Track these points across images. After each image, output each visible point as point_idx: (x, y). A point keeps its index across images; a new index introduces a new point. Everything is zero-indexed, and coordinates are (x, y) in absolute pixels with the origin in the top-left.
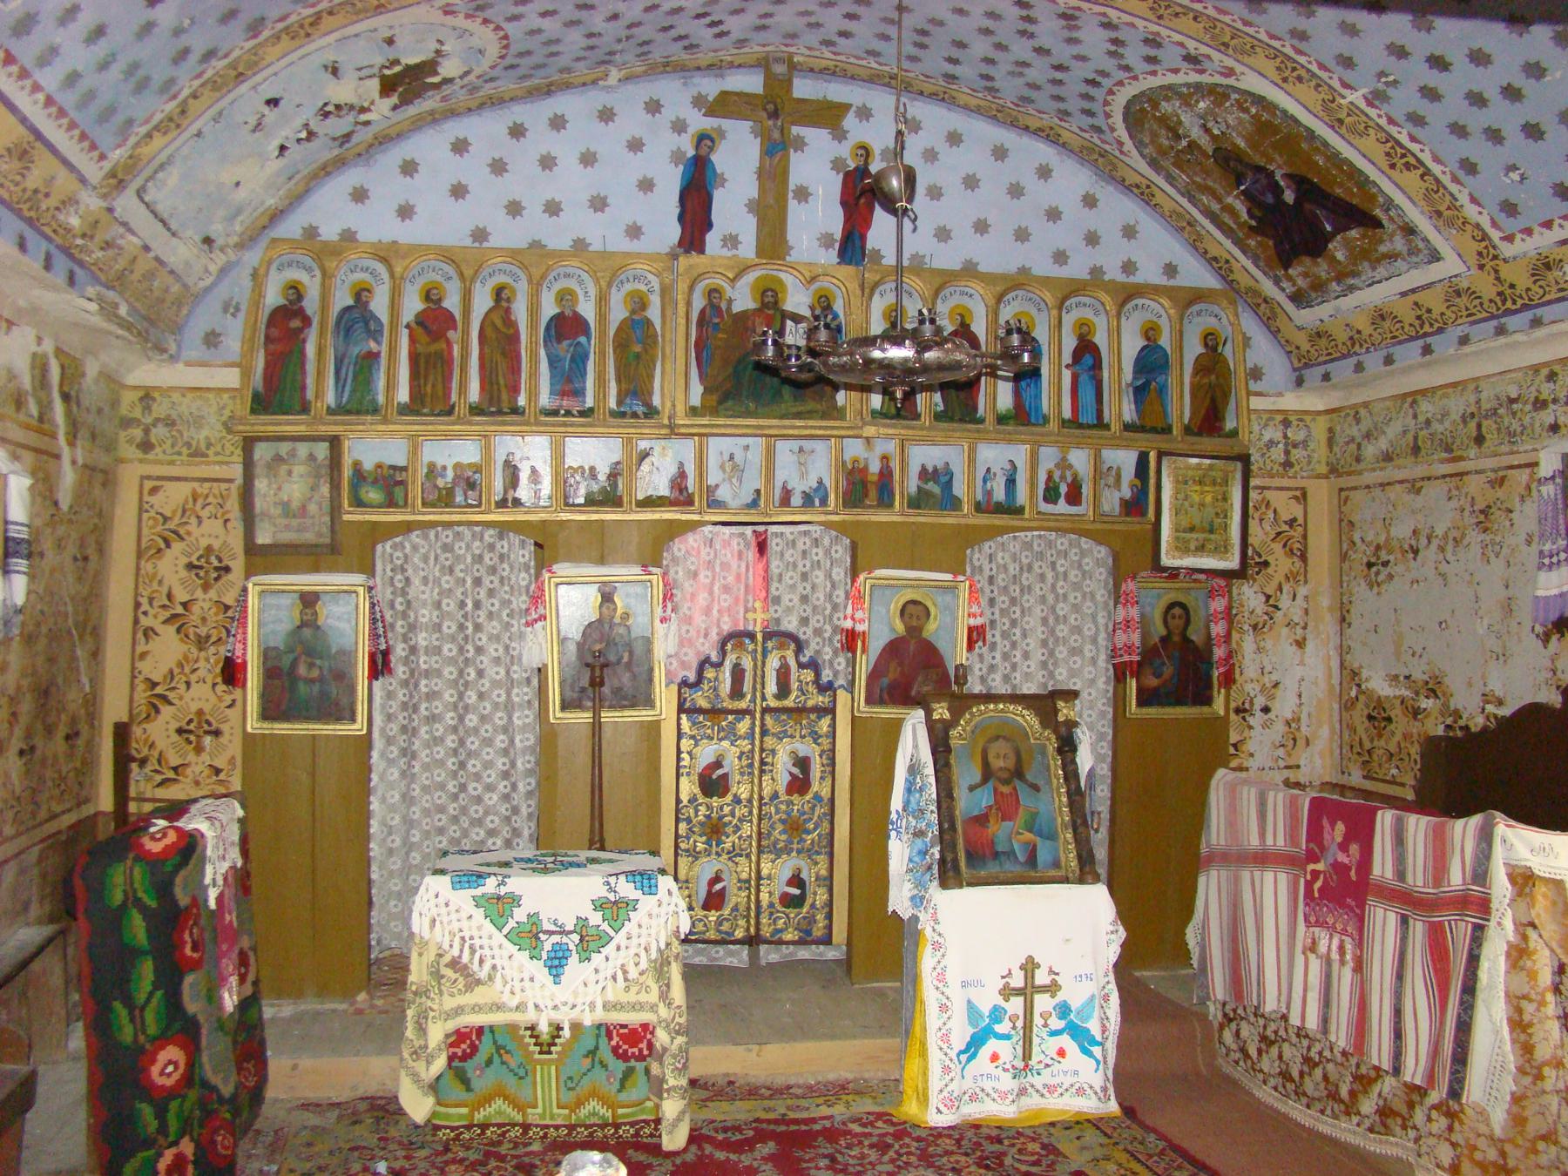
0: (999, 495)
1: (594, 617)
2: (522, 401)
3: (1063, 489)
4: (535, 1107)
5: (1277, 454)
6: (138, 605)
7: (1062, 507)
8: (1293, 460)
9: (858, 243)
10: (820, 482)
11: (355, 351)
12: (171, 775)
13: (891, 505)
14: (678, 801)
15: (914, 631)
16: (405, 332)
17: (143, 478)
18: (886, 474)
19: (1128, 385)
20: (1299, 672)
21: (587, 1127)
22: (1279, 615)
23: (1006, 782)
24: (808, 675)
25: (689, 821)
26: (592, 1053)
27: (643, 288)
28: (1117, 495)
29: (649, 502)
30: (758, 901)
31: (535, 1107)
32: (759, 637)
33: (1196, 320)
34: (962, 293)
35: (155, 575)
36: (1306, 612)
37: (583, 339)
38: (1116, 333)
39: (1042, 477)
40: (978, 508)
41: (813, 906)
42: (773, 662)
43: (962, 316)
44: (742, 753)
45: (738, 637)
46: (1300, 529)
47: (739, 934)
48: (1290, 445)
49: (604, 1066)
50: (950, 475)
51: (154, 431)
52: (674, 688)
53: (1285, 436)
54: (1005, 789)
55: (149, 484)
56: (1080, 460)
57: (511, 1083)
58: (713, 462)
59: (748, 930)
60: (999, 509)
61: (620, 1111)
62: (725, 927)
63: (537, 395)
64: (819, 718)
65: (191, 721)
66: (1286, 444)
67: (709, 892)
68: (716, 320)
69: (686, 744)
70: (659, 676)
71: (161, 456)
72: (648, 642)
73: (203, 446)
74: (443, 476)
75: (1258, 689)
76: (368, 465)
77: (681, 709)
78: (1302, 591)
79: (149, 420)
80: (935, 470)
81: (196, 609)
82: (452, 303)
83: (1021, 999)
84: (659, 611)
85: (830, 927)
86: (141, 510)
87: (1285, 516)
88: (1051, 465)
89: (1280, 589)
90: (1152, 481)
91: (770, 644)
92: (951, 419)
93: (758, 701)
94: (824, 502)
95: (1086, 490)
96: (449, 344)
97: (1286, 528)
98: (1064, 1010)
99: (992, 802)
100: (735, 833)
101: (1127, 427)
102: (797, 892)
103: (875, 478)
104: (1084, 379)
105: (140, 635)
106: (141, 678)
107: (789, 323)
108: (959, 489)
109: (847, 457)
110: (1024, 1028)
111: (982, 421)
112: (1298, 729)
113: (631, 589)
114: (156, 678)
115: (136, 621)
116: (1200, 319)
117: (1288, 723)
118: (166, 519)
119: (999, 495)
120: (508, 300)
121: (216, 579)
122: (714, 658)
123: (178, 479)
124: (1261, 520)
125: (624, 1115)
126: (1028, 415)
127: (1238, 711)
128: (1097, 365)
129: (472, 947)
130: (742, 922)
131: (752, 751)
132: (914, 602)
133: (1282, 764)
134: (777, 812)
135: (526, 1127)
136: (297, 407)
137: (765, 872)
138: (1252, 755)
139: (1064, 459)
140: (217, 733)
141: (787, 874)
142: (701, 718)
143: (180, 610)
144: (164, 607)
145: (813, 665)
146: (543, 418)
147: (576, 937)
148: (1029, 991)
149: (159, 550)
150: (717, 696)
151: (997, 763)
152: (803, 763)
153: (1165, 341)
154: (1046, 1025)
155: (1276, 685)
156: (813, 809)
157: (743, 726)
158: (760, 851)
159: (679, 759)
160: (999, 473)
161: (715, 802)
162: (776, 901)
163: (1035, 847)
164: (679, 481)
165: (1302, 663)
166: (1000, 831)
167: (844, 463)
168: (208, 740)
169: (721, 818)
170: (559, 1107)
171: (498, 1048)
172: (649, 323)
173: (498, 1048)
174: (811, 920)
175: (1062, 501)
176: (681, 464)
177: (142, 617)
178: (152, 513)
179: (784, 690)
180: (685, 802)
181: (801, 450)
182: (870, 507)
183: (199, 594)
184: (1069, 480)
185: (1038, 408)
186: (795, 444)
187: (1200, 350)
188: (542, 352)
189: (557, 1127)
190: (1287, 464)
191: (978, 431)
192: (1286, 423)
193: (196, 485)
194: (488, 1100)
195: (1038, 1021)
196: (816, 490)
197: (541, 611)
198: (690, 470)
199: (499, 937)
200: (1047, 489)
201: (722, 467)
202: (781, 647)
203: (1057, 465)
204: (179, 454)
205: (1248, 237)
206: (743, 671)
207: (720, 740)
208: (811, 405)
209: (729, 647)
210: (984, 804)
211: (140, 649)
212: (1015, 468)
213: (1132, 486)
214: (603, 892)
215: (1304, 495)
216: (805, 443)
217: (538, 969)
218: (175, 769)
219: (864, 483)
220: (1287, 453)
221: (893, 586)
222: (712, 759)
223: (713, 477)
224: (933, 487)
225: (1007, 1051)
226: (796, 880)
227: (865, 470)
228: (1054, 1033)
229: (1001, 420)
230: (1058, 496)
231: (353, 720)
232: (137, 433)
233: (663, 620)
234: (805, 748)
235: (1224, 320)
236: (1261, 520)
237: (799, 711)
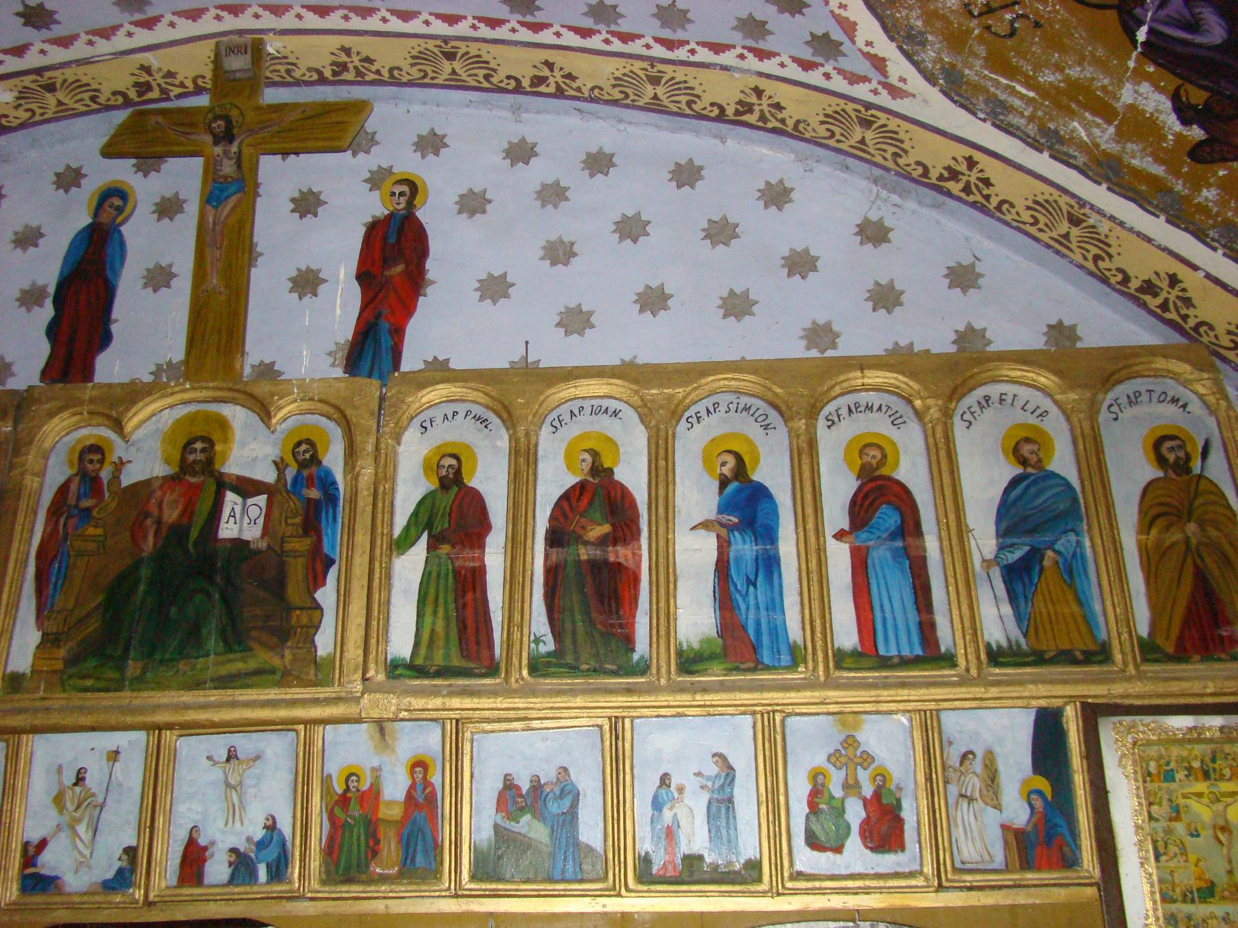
3: (855, 813)
7: (856, 856)
9: (386, 341)
10: (272, 827)
13: (434, 874)
28: (992, 819)
33: (1129, 413)
34: (595, 411)
39: (799, 790)
40: (647, 875)
43: (595, 454)
50: (569, 791)
68: (86, 503)
80: (537, 786)
88: (820, 760)
90: (1079, 780)
92: (574, 670)
94: (278, 871)
95: (912, 812)
101: (996, 656)
103: (396, 813)
104: (881, 555)
107: (230, 497)
108: (591, 830)
109: (334, 767)
111: (643, 668)
116: (1135, 410)
126: (755, 649)
128: (910, 527)
139: (850, 742)
153: (1062, 462)
160: (691, 784)
167: (326, 780)
175: (854, 843)
181: (232, 756)
182: (384, 879)
184: (868, 791)
185: (778, 631)
186: (218, 744)
187: (1149, 472)
196: (261, 845)
201: (59, 800)
203: (833, 758)
205: (1197, 184)
208: (262, 657)
212: (729, 770)
213: (1030, 795)
216: (239, 740)
219: (372, 826)
224: (531, 828)
227: (372, 796)
229: (690, 662)
235: (1196, 407)
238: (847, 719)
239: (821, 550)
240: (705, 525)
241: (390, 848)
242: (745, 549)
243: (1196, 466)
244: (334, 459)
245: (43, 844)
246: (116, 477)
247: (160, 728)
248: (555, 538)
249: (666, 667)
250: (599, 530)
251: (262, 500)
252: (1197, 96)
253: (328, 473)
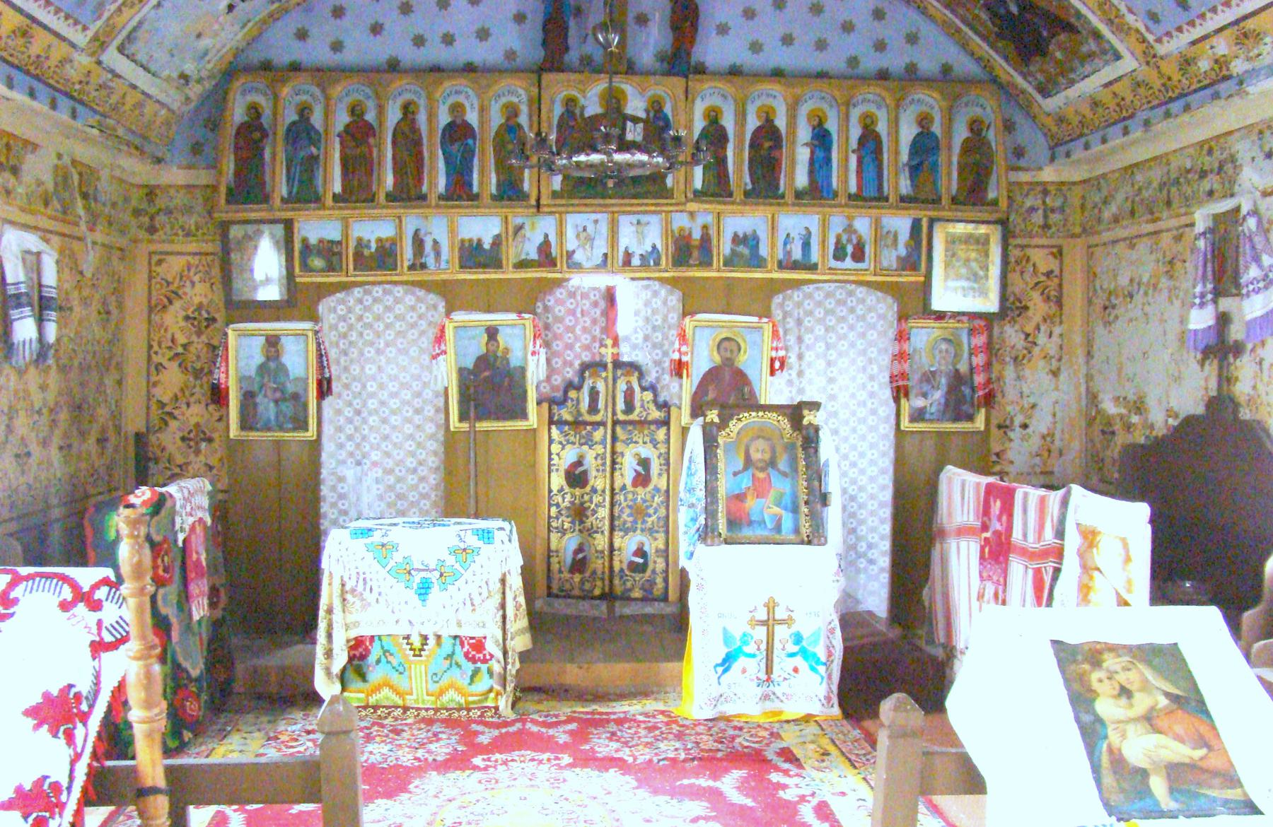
0: (797, 254)
1: (484, 350)
2: (425, 189)
3: (850, 249)
4: (411, 694)
5: (1038, 218)
6: (150, 347)
7: (849, 263)
8: (1050, 222)
10: (654, 247)
11: (302, 154)
12: (177, 470)
13: (709, 264)
14: (550, 491)
15: (728, 362)
16: (337, 140)
17: (150, 254)
18: (706, 240)
19: (904, 165)
20: (1055, 395)
21: (448, 710)
22: (1036, 350)
23: (763, 469)
24: (648, 396)
25: (558, 505)
26: (450, 656)
27: (515, 100)
28: (894, 254)
29: (522, 265)
30: (611, 567)
31: (411, 694)
32: (610, 366)
34: (768, 95)
35: (162, 326)
36: (1061, 347)
37: (470, 142)
38: (895, 124)
39: (832, 241)
40: (781, 266)
41: (654, 572)
42: (622, 386)
43: (767, 113)
45: (594, 366)
46: (1056, 281)
47: (597, 592)
48: (1048, 211)
49: (458, 665)
50: (756, 238)
51: (158, 218)
52: (545, 405)
53: (1044, 202)
54: (761, 475)
55: (155, 258)
56: (863, 225)
57: (395, 678)
58: (570, 233)
59: (603, 589)
60: (795, 266)
61: (471, 699)
62: (587, 586)
63: (436, 185)
65: (190, 431)
66: (1045, 211)
67: (574, 559)
68: (571, 123)
69: (555, 448)
70: (532, 396)
71: (164, 237)
72: (523, 370)
73: (193, 228)
74: (369, 247)
75: (1018, 408)
76: (313, 240)
77: (551, 422)
78: (1057, 330)
79: (153, 210)
80: (745, 236)
81: (192, 349)
82: (370, 117)
83: (765, 628)
84: (531, 348)
85: (666, 588)
86: (150, 278)
87: (1043, 268)
88: (840, 231)
89: (1038, 328)
90: (924, 243)
91: (619, 372)
92: (758, 196)
93: (610, 415)
94: (657, 263)
95: (869, 250)
96: (370, 147)
97: (1043, 278)
98: (798, 639)
99: (750, 484)
101: (903, 199)
102: (641, 561)
103: (697, 243)
105: (153, 368)
106: (154, 400)
108: (764, 251)
110: (767, 650)
112: (1053, 442)
113: (509, 331)
114: (165, 399)
115: (149, 357)
117: (1044, 437)
118: (168, 284)
119: (797, 254)
120: (413, 113)
121: (207, 327)
122: (576, 380)
123: (179, 253)
124: (1022, 273)
125: (474, 702)
126: (821, 191)
127: (1000, 427)
128: (878, 150)
129: (364, 579)
130: (599, 583)
131: (604, 453)
132: (727, 339)
133: (1038, 470)
135: (406, 709)
136: (260, 197)
137: (616, 545)
138: (1012, 462)
139: (850, 226)
140: (210, 440)
141: (634, 547)
142: (566, 428)
143: (180, 350)
144: (170, 348)
145: (653, 388)
146: (442, 203)
147: (437, 574)
148: (771, 622)
149: (164, 307)
150: (578, 411)
151: (756, 456)
152: (645, 463)
153: (936, 128)
154: (783, 649)
155: (1033, 406)
156: (653, 497)
157: (598, 435)
158: (612, 529)
159: (550, 459)
160: (797, 237)
161: (578, 491)
162: (625, 566)
163: (780, 519)
164: (545, 248)
165: (1057, 389)
166: (752, 504)
168: (203, 445)
169: (582, 504)
170: (428, 695)
171: (385, 652)
172: (520, 126)
173: (385, 652)
174: (652, 583)
175: (848, 259)
176: (546, 236)
177: (154, 356)
178: (159, 279)
179: (629, 408)
180: (555, 491)
181: (639, 223)
183: (194, 338)
184: (855, 241)
185: (829, 184)
186: (634, 218)
188: (440, 152)
189: (427, 710)
190: (1046, 226)
191: (779, 204)
192: (1045, 192)
193: (190, 258)
194: (378, 689)
195: (777, 645)
197: (443, 347)
198: (552, 238)
199: (383, 572)
200: (836, 249)
201: (578, 236)
202: (628, 374)
204: (176, 234)
206: (598, 393)
207: (581, 445)
209: (587, 374)
210: (744, 486)
211: (154, 378)
212: (809, 233)
213: (907, 246)
214: (456, 542)
215: (1060, 252)
217: (412, 596)
218: (180, 466)
220: (1046, 217)
221: (711, 326)
223: (571, 243)
225: (755, 666)
226: (640, 552)
228: (792, 655)
229: (799, 195)
230: (846, 255)
231: (307, 430)
232: (146, 220)
233: (534, 353)
234: (646, 451)
235: (989, 109)
236: (1022, 273)
237: (642, 423)
238: (850, 218)
239: (847, 159)
240: (806, 144)
241: (695, 253)
242: (820, 154)
243: (984, 133)
244: (668, 110)
245: (574, 252)
246: (582, 114)
247: (613, 213)
248: (751, 146)
249: (790, 198)
250: (767, 145)
251: (641, 125)
252: (998, 22)
253: (666, 115)
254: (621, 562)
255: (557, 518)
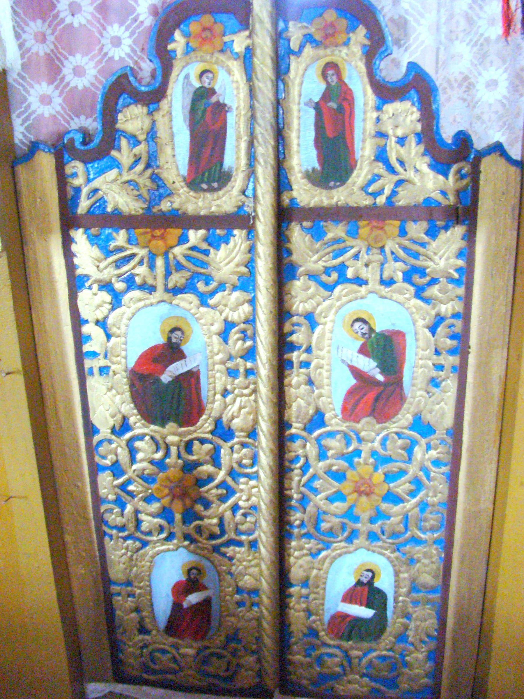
41: (401, 637)
44: (229, 325)
64: (432, 233)
67: (177, 606)
100: (223, 499)
102: (366, 613)
131: (251, 320)
134: (322, 455)
150: (156, 178)
156: (409, 449)
180: (105, 432)
207: (176, 291)
222: (159, 339)
254: (309, 612)
255: (120, 503)
